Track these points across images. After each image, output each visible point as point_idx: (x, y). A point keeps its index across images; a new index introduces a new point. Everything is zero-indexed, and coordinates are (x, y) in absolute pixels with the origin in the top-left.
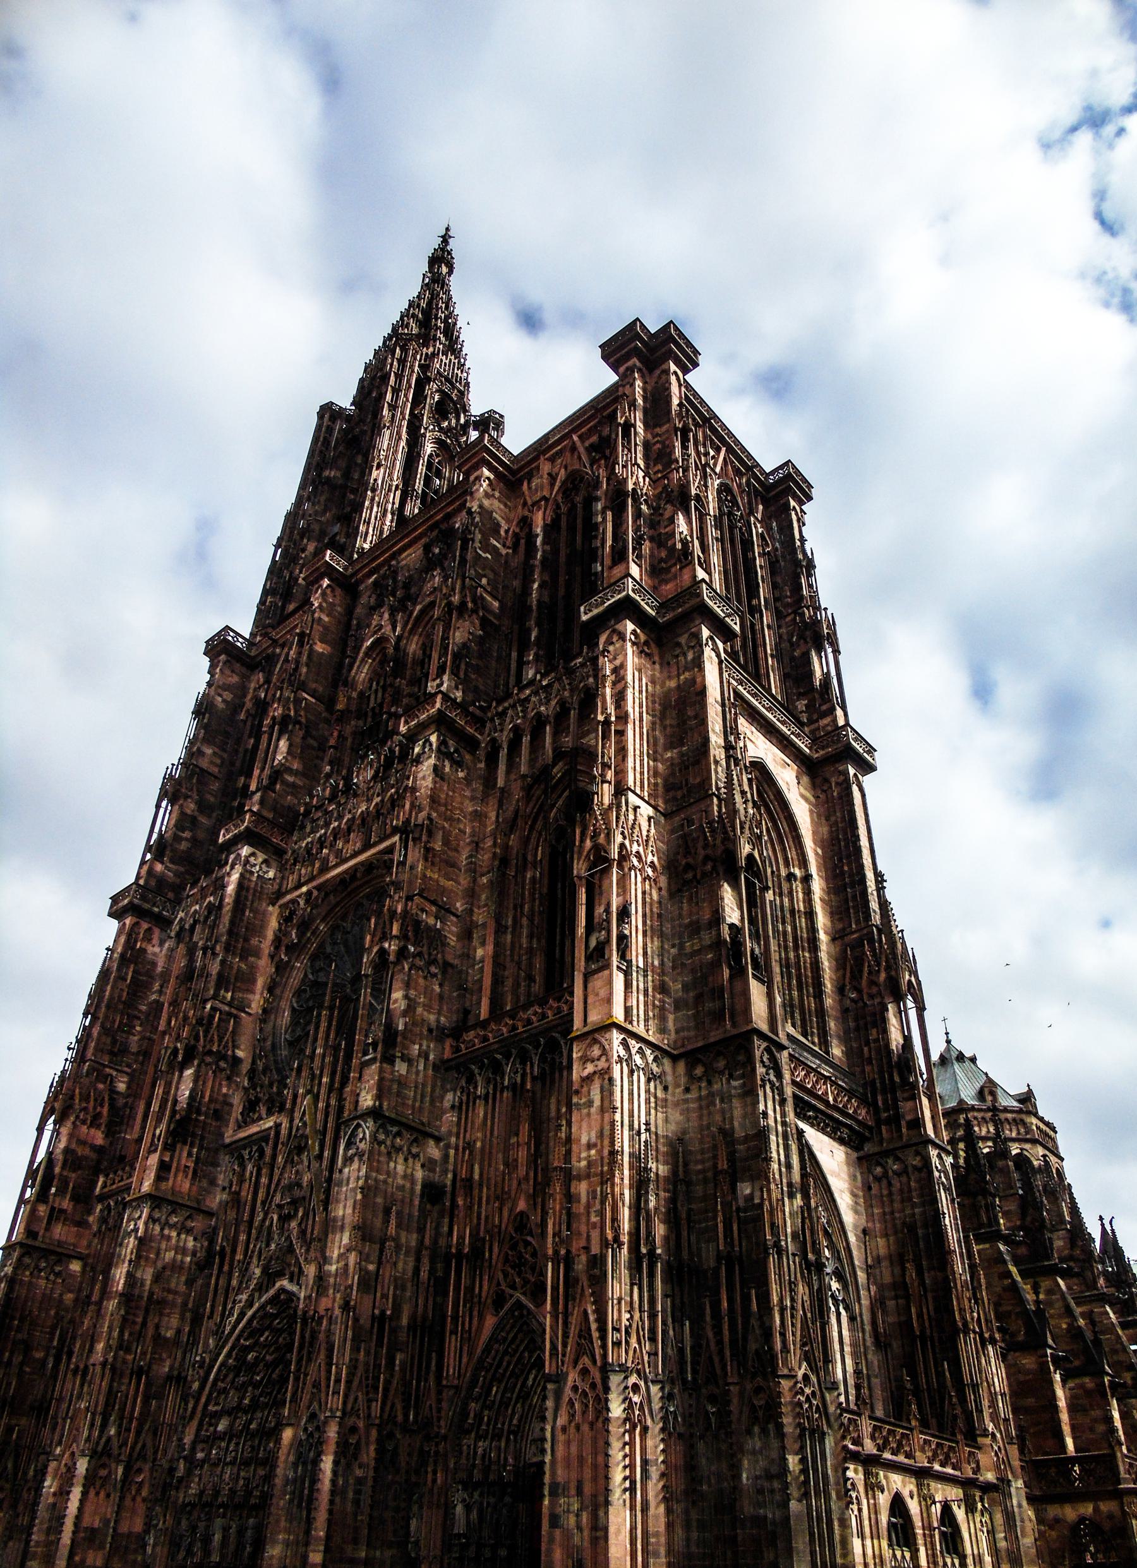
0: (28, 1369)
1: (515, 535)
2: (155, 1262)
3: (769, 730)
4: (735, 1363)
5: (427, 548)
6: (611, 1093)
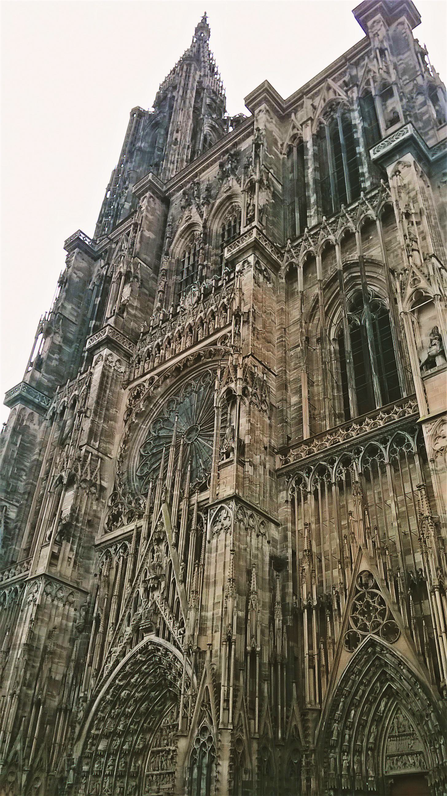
2: (48, 624)
5: (221, 166)
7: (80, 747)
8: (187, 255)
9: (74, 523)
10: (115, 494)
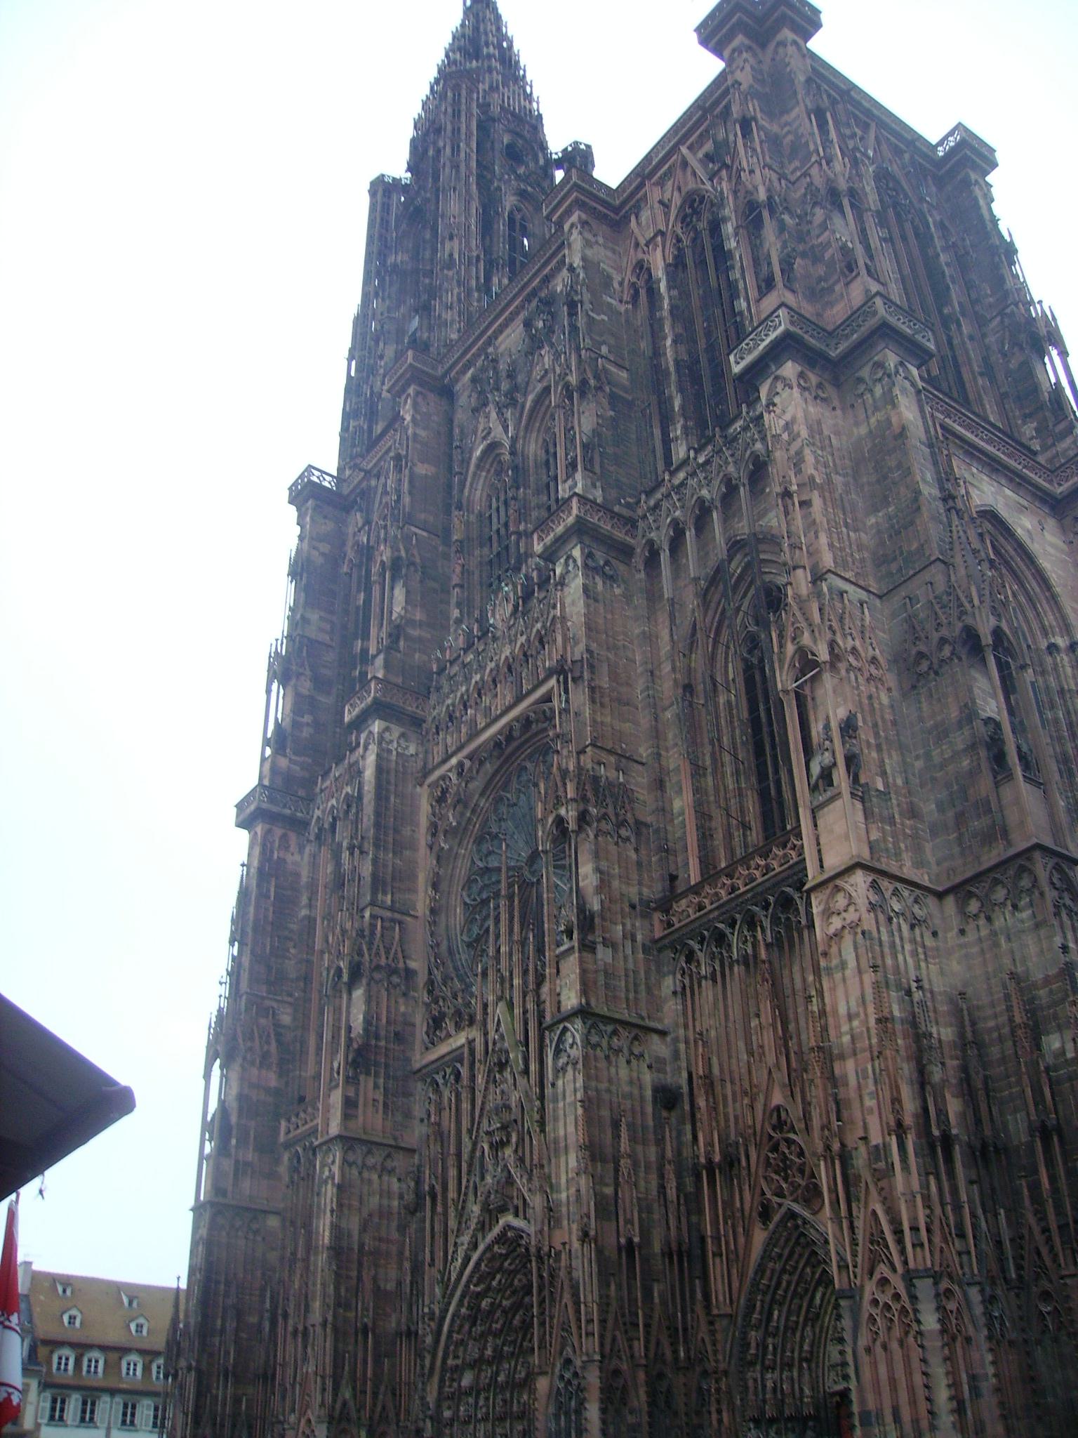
1: (633, 285)
3: (994, 467)
4: (1068, 1252)
5: (528, 324)
7: (436, 1386)
8: (494, 505)
9: (373, 1042)
10: (431, 983)
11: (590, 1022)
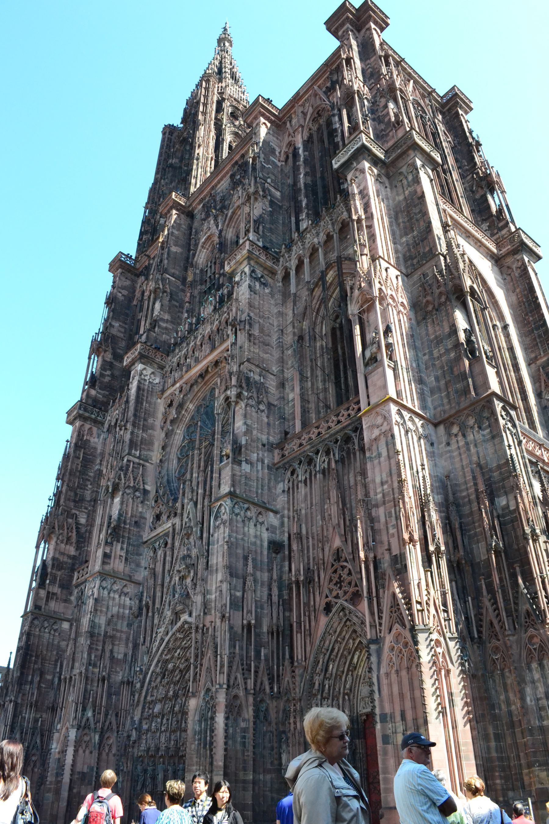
0: (44, 686)
1: (286, 153)
4: (511, 621)
5: (232, 176)
6: (394, 444)
8: (209, 265)
9: (123, 525)
11: (235, 501)
